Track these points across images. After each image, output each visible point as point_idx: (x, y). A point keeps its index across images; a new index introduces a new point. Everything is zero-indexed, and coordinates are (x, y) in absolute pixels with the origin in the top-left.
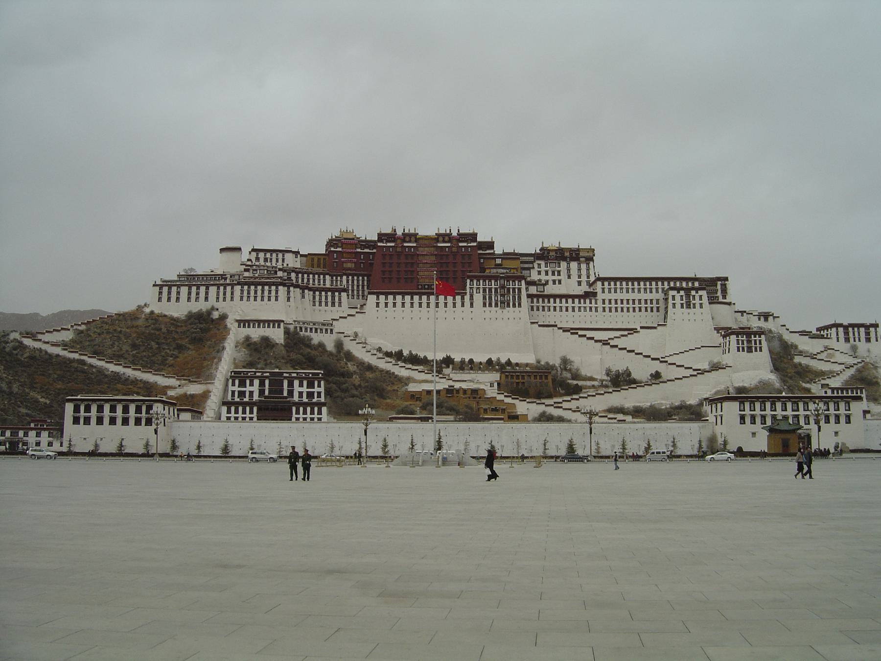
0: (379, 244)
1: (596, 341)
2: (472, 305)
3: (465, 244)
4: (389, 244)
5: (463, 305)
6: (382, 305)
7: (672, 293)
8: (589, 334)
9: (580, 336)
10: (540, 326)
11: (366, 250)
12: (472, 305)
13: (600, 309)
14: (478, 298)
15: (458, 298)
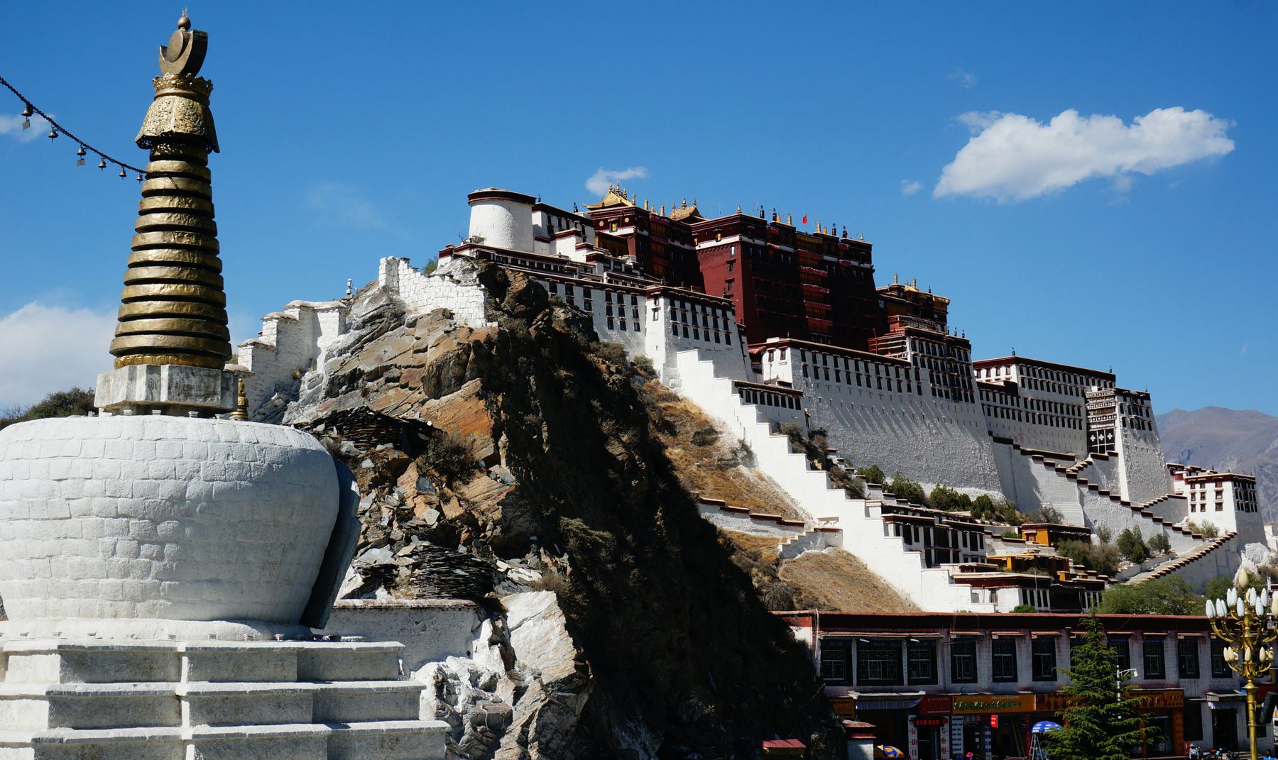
0: (745, 239)
1: (1070, 477)
2: (920, 393)
3: (856, 263)
4: (757, 242)
5: (909, 390)
6: (810, 370)
7: (1118, 401)
8: (1060, 464)
9: (1048, 465)
10: (997, 440)
11: (677, 244)
12: (920, 393)
13: (1023, 415)
14: (924, 373)
15: (902, 371)
